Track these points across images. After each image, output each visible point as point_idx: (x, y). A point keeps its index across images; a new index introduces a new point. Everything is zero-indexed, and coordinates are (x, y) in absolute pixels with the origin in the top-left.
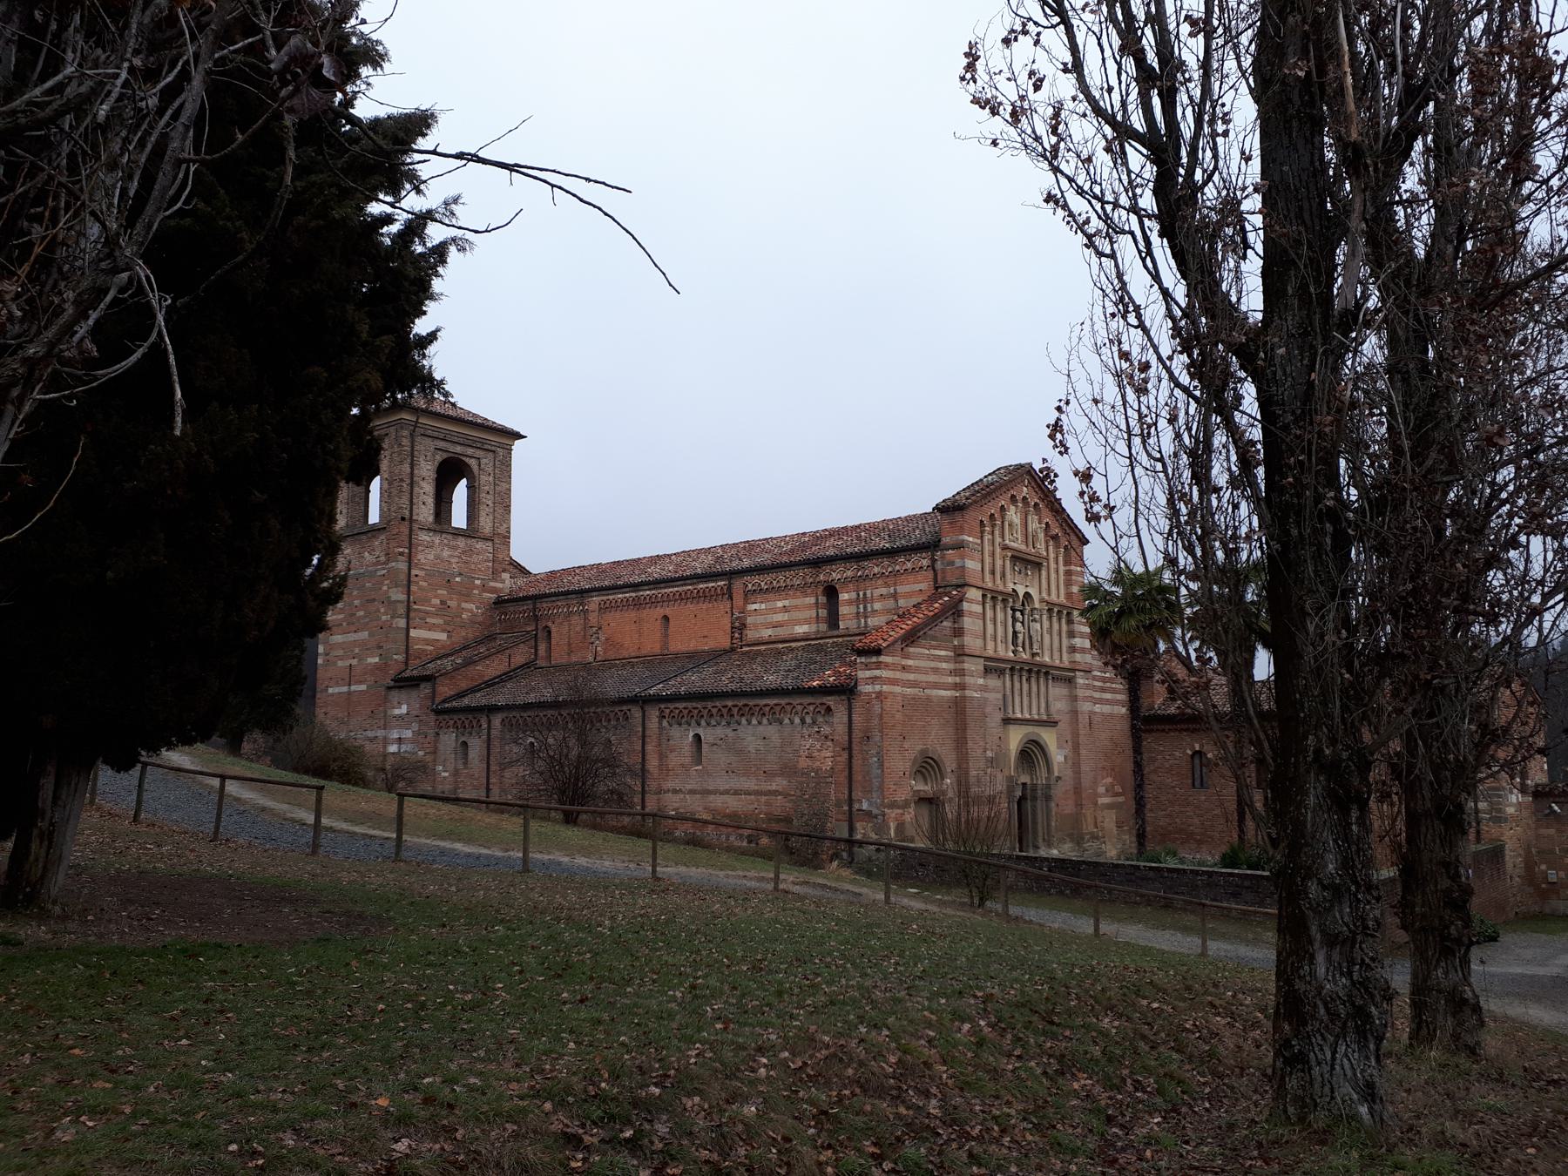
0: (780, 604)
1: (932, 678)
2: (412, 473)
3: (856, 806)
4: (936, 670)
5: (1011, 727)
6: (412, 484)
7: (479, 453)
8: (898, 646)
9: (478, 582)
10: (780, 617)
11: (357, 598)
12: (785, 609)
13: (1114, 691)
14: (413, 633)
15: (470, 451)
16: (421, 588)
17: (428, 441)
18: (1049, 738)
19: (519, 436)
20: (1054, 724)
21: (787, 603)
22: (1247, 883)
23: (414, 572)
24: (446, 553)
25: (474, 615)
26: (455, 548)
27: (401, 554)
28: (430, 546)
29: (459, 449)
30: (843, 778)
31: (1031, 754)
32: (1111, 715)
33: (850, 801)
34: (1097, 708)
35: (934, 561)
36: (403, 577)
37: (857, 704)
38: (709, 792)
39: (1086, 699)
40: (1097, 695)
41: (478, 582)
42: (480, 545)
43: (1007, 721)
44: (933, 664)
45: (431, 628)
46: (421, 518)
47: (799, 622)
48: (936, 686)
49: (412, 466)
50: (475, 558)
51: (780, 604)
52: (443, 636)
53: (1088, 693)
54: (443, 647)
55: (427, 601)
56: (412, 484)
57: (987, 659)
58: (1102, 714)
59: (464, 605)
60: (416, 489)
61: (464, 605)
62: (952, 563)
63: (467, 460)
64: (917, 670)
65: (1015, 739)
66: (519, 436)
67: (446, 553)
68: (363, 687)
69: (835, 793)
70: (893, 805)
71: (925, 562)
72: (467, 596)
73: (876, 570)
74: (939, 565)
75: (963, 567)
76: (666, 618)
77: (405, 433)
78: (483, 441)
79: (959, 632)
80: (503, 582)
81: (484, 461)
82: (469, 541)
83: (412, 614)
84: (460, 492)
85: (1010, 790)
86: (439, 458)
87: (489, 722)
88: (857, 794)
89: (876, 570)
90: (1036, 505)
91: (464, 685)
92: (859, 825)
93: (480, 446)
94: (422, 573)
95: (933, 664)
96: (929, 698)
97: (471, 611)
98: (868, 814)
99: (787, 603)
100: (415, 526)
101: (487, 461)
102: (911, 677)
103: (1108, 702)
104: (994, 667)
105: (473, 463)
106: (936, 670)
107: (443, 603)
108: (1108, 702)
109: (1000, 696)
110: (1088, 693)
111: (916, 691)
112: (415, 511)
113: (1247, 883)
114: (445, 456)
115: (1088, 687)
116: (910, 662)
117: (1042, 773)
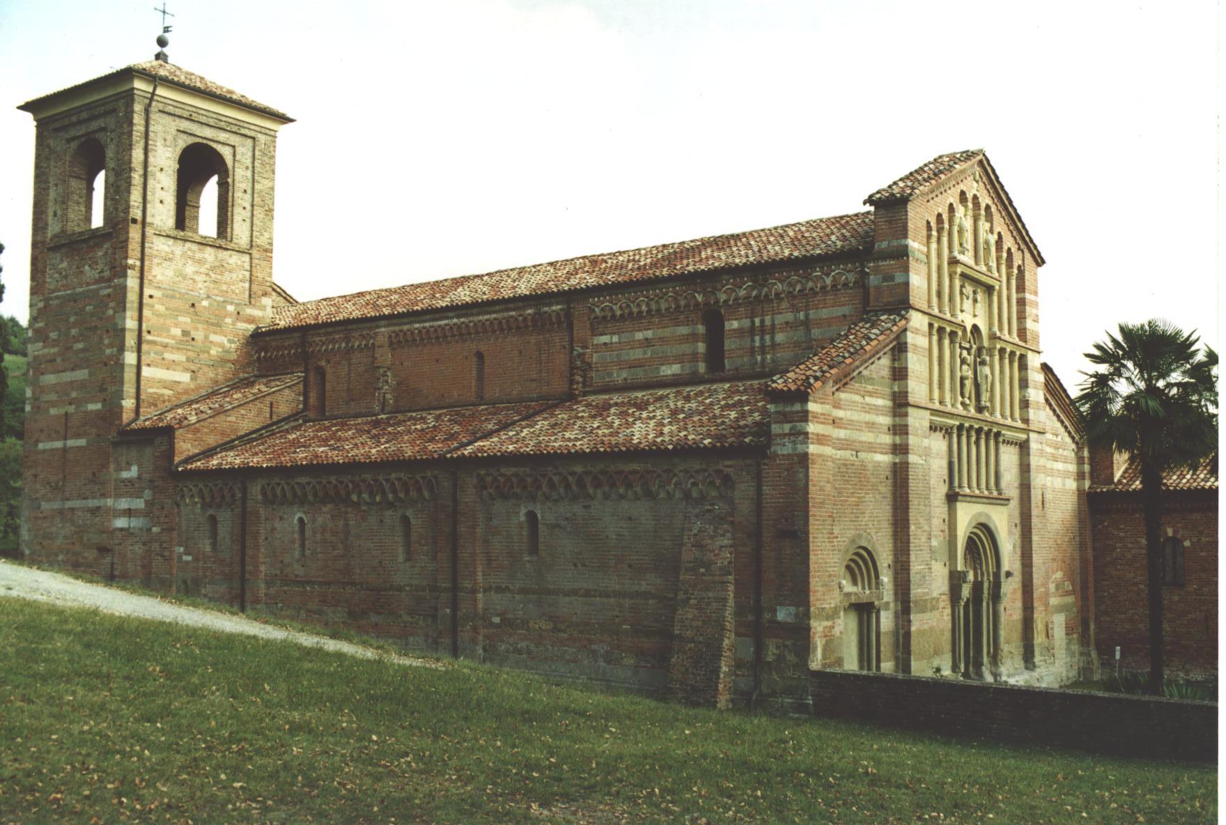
0: (640, 336)
10: (637, 354)
11: (75, 325)
12: (647, 342)
14: (146, 372)
15: (222, 136)
16: (159, 315)
19: (284, 119)
21: (649, 334)
23: (147, 292)
24: (190, 269)
25: (227, 351)
26: (200, 262)
29: (208, 133)
35: (864, 275)
41: (231, 308)
47: (666, 361)
50: (227, 277)
51: (640, 336)
52: (185, 378)
54: (186, 392)
55: (165, 329)
57: (934, 412)
59: (213, 337)
60: (151, 182)
61: (213, 337)
63: (214, 145)
64: (849, 425)
67: (190, 269)
68: (82, 442)
71: (852, 277)
72: (216, 325)
76: (480, 355)
80: (263, 308)
81: (239, 150)
82: (223, 254)
83: (145, 347)
84: (210, 192)
87: (244, 491)
89: (779, 287)
90: (988, 207)
91: (212, 440)
93: (235, 129)
97: (221, 345)
99: (649, 334)
100: (149, 231)
102: (842, 433)
105: (226, 152)
107: (185, 333)
114: (191, 140)
116: (840, 413)
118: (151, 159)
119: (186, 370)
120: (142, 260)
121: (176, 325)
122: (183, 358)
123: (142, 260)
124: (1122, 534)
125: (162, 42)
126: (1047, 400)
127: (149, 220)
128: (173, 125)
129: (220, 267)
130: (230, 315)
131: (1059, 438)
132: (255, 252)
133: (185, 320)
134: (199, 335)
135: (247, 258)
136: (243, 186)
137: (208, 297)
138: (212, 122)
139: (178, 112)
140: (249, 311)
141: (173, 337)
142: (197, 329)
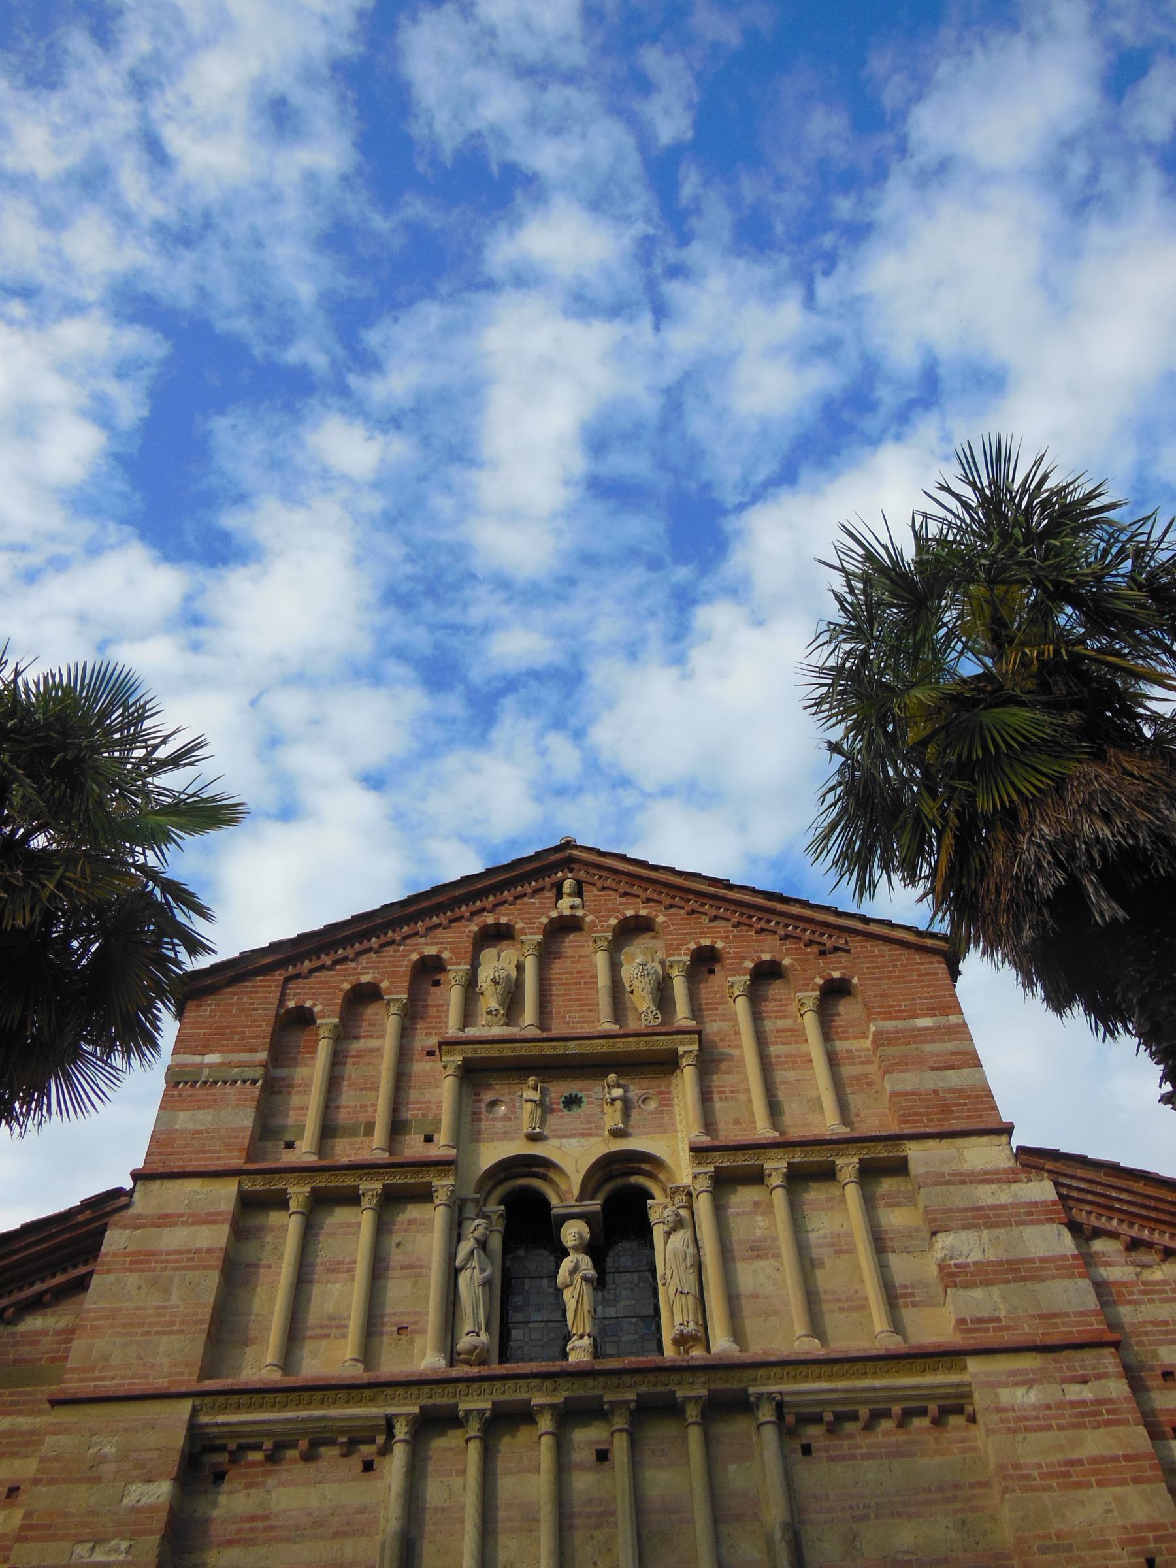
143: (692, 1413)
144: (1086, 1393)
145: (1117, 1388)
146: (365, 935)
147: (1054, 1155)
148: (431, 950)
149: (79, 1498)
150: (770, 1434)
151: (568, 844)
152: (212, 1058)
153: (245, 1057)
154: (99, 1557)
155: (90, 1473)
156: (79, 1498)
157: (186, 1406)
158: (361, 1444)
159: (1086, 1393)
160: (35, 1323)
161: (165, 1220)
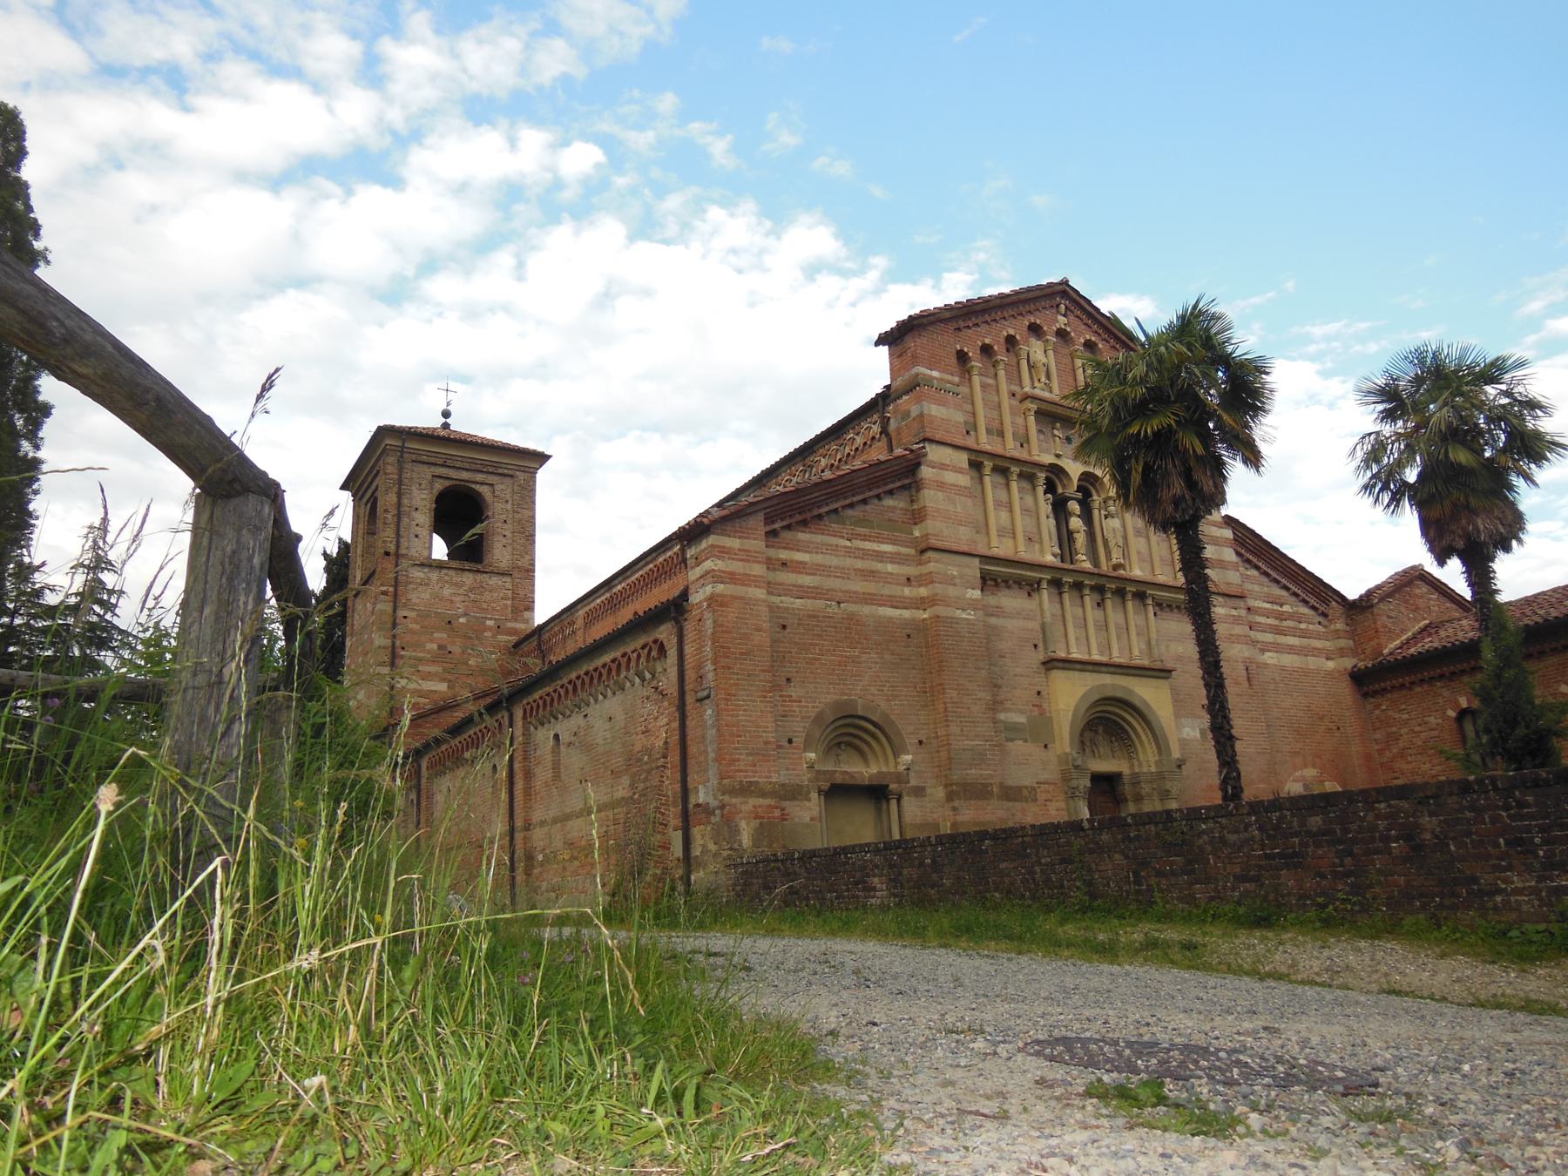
1: (858, 586)
2: (399, 504)
3: (692, 800)
4: (870, 575)
5: (1057, 675)
6: (399, 516)
7: (491, 479)
8: (757, 523)
9: (490, 623)
13: (1304, 634)
15: (480, 477)
16: (412, 632)
17: (424, 468)
18: (1150, 694)
19: (542, 458)
20: (1164, 673)
22: (1315, 822)
23: (401, 613)
24: (447, 592)
26: (457, 585)
27: (383, 593)
28: (425, 583)
29: (465, 475)
30: (674, 757)
31: (1110, 722)
32: (1305, 672)
33: (685, 792)
34: (1269, 658)
35: (885, 423)
36: (388, 620)
37: (689, 627)
38: (566, 818)
39: (1234, 639)
40: (1269, 637)
42: (494, 581)
43: (1051, 664)
44: (860, 564)
45: (426, 677)
46: (413, 553)
48: (869, 599)
49: (399, 495)
50: (487, 596)
52: (443, 687)
53: (1238, 630)
56: (399, 516)
58: (1283, 668)
60: (405, 520)
62: (907, 414)
63: (477, 487)
64: (816, 570)
65: (1069, 696)
66: (542, 458)
67: (447, 592)
69: (671, 787)
70: (746, 790)
71: (876, 429)
73: (823, 462)
74: (893, 425)
75: (921, 415)
77: (391, 459)
78: (497, 465)
79: (918, 517)
82: (479, 577)
85: (1066, 778)
86: (439, 486)
88: (692, 778)
89: (823, 462)
92: (696, 832)
94: (412, 614)
95: (860, 564)
96: (851, 618)
98: (707, 810)
101: (503, 487)
102: (807, 580)
103: (1291, 650)
104: (999, 575)
106: (870, 575)
107: (441, 647)
108: (1291, 650)
109: (1035, 625)
110: (1238, 630)
111: (820, 603)
112: (404, 542)
113: (1315, 822)
114: (447, 483)
115: (1237, 620)
117: (1148, 759)
118: (405, 501)
119: (444, 680)
120: (396, 586)
121: (431, 641)
122: (440, 670)
123: (396, 586)
124: (1405, 716)
125: (446, 414)
126: (1238, 554)
127: (403, 551)
128: (428, 472)
129: (481, 588)
130: (490, 629)
131: (1286, 608)
132: (516, 574)
133: (441, 636)
134: (456, 649)
135: (508, 579)
136: (504, 517)
137: (466, 615)
138: (467, 466)
139: (432, 460)
140: (510, 625)
141: (429, 652)
142: (453, 643)
143: (1129, 596)
144: (1234, 612)
145: (1243, 612)
146: (984, 311)
147: (1236, 521)
148: (1012, 332)
149: (952, 591)
150: (1151, 609)
151: (1065, 283)
152: (935, 374)
153: (949, 377)
154: (964, 616)
155: (950, 581)
156: (952, 591)
157: (977, 561)
158: (1032, 587)
159: (1234, 612)
160: (889, 502)
161: (943, 467)
